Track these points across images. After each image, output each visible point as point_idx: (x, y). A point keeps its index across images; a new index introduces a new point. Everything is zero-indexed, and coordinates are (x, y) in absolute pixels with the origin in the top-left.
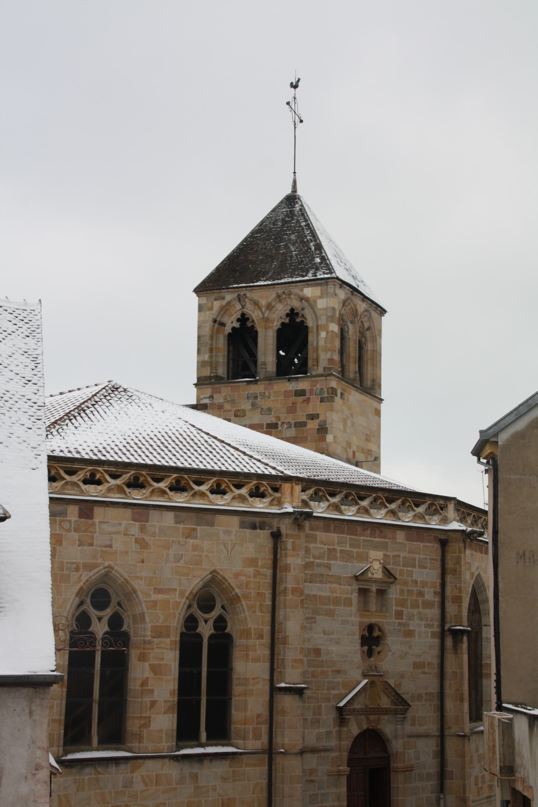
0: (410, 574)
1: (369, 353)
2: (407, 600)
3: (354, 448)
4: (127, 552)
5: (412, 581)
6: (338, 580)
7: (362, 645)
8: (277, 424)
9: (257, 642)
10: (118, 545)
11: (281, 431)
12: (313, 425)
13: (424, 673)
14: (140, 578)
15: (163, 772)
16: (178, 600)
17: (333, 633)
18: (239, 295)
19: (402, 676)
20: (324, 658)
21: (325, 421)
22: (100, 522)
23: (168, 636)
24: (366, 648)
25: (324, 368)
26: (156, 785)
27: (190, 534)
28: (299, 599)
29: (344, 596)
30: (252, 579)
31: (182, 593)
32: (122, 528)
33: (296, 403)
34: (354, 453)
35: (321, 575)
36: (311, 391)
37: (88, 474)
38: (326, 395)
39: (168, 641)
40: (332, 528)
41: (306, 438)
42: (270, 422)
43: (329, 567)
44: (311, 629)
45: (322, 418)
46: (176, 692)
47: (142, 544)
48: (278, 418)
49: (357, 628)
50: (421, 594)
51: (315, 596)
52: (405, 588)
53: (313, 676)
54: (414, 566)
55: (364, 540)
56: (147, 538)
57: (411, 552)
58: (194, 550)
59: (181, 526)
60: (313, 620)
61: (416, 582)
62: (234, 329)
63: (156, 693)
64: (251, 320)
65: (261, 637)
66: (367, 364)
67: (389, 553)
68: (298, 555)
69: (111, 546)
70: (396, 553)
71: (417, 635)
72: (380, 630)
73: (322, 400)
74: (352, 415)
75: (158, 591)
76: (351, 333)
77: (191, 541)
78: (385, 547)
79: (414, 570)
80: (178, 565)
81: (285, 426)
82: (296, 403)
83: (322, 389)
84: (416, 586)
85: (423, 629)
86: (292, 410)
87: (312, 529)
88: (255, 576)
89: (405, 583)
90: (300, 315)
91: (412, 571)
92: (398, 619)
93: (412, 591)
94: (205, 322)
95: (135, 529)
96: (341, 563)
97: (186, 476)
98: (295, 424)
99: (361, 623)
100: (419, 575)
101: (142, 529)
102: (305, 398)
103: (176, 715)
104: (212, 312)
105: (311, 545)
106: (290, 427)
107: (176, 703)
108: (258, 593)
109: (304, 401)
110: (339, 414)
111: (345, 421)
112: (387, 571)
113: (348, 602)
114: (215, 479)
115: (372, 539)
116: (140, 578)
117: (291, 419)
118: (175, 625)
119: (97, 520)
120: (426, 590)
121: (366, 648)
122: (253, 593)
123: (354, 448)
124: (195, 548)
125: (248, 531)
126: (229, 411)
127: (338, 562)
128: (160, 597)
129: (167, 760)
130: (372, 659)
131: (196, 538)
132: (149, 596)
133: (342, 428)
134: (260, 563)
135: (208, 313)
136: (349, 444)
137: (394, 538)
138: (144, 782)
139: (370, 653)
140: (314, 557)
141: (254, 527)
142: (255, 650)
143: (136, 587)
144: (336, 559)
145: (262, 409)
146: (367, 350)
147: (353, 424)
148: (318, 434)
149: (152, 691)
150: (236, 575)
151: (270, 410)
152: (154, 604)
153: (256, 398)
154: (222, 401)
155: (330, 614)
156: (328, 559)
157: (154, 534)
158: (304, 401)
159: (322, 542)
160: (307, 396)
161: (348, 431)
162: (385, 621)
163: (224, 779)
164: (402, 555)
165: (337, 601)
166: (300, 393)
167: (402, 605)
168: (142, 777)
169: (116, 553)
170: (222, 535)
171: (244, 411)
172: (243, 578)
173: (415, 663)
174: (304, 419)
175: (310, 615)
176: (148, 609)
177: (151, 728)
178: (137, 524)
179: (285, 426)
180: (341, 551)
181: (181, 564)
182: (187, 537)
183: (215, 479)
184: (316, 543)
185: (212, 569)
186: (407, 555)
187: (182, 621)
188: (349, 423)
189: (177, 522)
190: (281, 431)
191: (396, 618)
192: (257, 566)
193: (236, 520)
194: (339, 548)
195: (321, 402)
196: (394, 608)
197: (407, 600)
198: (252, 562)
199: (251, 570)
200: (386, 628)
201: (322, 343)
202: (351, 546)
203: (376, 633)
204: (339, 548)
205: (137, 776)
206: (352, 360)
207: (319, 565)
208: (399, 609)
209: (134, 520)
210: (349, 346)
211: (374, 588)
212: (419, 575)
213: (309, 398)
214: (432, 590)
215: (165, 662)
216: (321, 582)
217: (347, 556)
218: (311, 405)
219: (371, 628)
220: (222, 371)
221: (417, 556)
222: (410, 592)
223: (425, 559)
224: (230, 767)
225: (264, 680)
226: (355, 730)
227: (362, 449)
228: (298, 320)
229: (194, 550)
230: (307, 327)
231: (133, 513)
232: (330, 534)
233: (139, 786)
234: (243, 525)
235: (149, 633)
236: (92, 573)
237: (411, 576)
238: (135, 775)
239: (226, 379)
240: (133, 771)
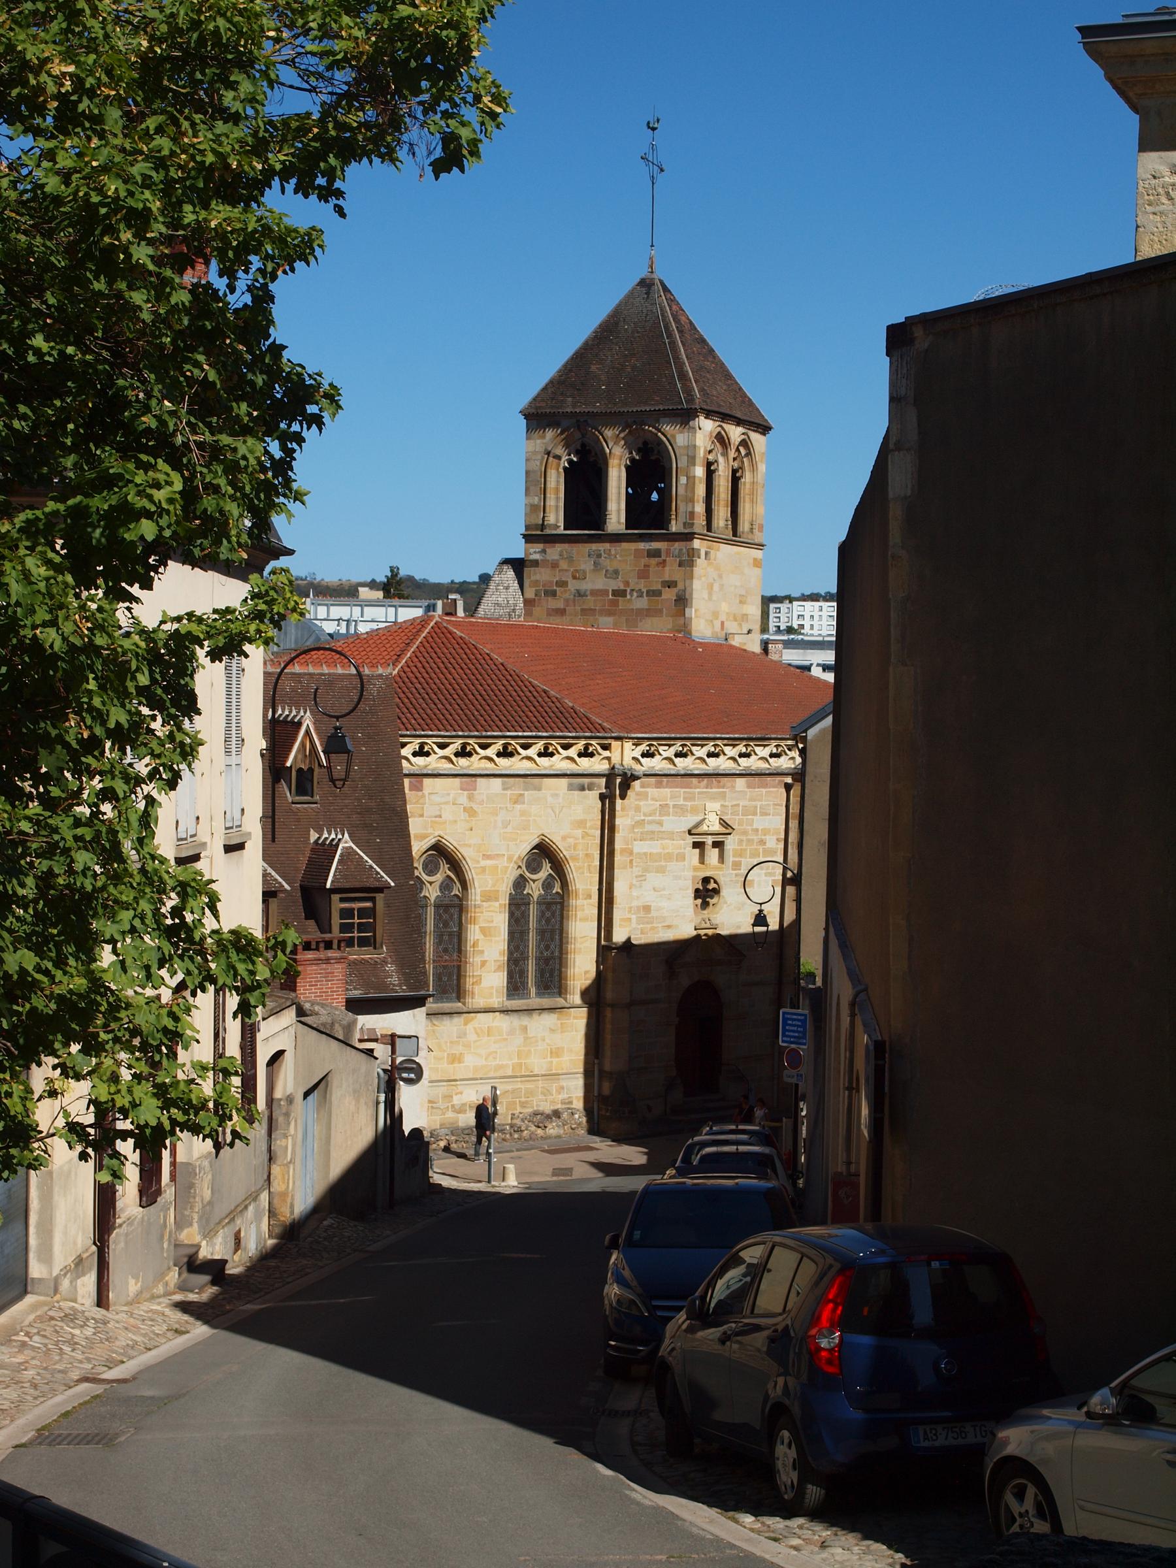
0: (751, 823)
1: (748, 486)
2: (746, 850)
3: (723, 617)
4: (456, 821)
5: (752, 830)
6: (671, 835)
7: (696, 898)
8: (626, 590)
9: (585, 902)
10: (447, 815)
11: (630, 600)
12: (669, 595)
14: (470, 846)
15: (494, 1025)
16: (506, 864)
17: (664, 889)
18: (578, 421)
20: (653, 914)
21: (684, 591)
22: (430, 794)
23: (497, 899)
24: (699, 901)
25: (685, 524)
26: (488, 1035)
27: (518, 800)
28: (628, 859)
29: (676, 852)
30: (581, 841)
31: (510, 858)
32: (451, 798)
33: (648, 566)
34: (722, 623)
35: (653, 832)
36: (668, 552)
37: (417, 747)
38: (685, 558)
39: (497, 904)
40: (664, 783)
41: (661, 611)
42: (616, 588)
43: (660, 823)
44: (641, 887)
45: (680, 586)
46: (506, 952)
47: (471, 812)
48: (627, 584)
49: (690, 882)
50: (762, 842)
51: (645, 854)
52: (744, 838)
53: (642, 933)
54: (755, 814)
56: (475, 807)
57: (751, 800)
58: (521, 815)
59: (509, 792)
60: (643, 878)
61: (757, 830)
62: (570, 462)
63: (486, 953)
64: (593, 454)
65: (590, 897)
66: (744, 502)
67: (727, 803)
68: (628, 815)
69: (440, 816)
70: (735, 803)
71: (755, 885)
72: (715, 882)
73: (680, 566)
74: (720, 576)
75: (487, 857)
76: (721, 468)
77: (518, 807)
78: (723, 796)
79: (755, 818)
80: (505, 830)
81: (635, 594)
82: (648, 566)
83: (681, 550)
84: (757, 835)
85: (764, 878)
86: (643, 574)
87: (642, 786)
88: (583, 837)
89: (745, 833)
90: (656, 452)
91: (753, 820)
92: (735, 870)
93: (753, 840)
94: (535, 452)
95: (463, 798)
96: (674, 818)
97: (512, 742)
98: (648, 592)
99: (694, 878)
100: (760, 822)
101: (470, 798)
102: (660, 560)
103: (506, 973)
104: (544, 441)
105: (642, 803)
106: (641, 596)
107: (506, 962)
108: (587, 855)
109: (658, 564)
110: (703, 579)
111: (710, 587)
112: (724, 823)
113: (681, 857)
114: (543, 742)
115: (709, 790)
116: (470, 846)
117: (642, 585)
118: (504, 889)
119: (426, 791)
120: (767, 837)
121: (699, 901)
122: (581, 854)
123: (723, 617)
124: (523, 813)
125: (576, 792)
126: (567, 570)
127: (671, 817)
128: (488, 862)
129: (497, 1014)
130: (705, 912)
131: (524, 803)
132: (478, 862)
133: (706, 596)
134: (588, 825)
135: (538, 441)
136: (716, 614)
137: (733, 787)
138: (477, 1033)
139: (705, 905)
140: (645, 815)
141: (582, 789)
142: (583, 910)
143: (465, 855)
144: (669, 815)
145: (607, 571)
146: (745, 483)
147: (722, 586)
148: (675, 605)
149: (482, 952)
150: (564, 838)
151: (616, 572)
152: (483, 869)
153: (599, 556)
154: (556, 557)
155: (661, 870)
156: (660, 815)
157: (482, 802)
158: (658, 564)
159: (653, 799)
160: (663, 557)
161: (714, 598)
162: (721, 873)
163: (552, 1031)
164: (741, 804)
165: (668, 857)
166: (656, 554)
167: (741, 856)
168: (475, 1028)
169: (445, 823)
170: (550, 799)
171: (584, 572)
172: (571, 840)
174: (659, 587)
175: (640, 873)
176: (477, 874)
177: (482, 985)
178: (466, 792)
179: (635, 594)
180: (674, 806)
181: (509, 829)
182: (515, 803)
183: (543, 742)
184: (647, 800)
185: (540, 833)
186: (746, 803)
187: (511, 884)
188: (716, 587)
189: (504, 789)
190: (630, 600)
191: (733, 869)
192: (585, 828)
193: (564, 782)
194: (671, 804)
195: (680, 566)
196: (731, 859)
197: (746, 850)
198: (581, 824)
199: (579, 833)
200: (721, 880)
201: (681, 491)
202: (685, 799)
203: (712, 885)
204: (671, 804)
205: (470, 1027)
206: (722, 503)
207: (650, 822)
208: (737, 859)
209: (462, 789)
210: (719, 485)
211: (709, 840)
212: (760, 822)
213: (664, 561)
214: (775, 837)
215: (494, 924)
216: (652, 839)
217: (681, 810)
218: (667, 568)
219: (706, 880)
220: (556, 517)
221: (759, 804)
222: (750, 841)
223: (769, 805)
224: (558, 1019)
225: (592, 938)
226: (685, 981)
227: (734, 615)
228: (653, 458)
229: (521, 815)
230: (663, 467)
231: (461, 783)
232: (662, 790)
233: (472, 1037)
234: (571, 788)
235: (478, 898)
236: (423, 843)
237: (752, 825)
238: (468, 1027)
239: (562, 528)
240: (466, 1024)
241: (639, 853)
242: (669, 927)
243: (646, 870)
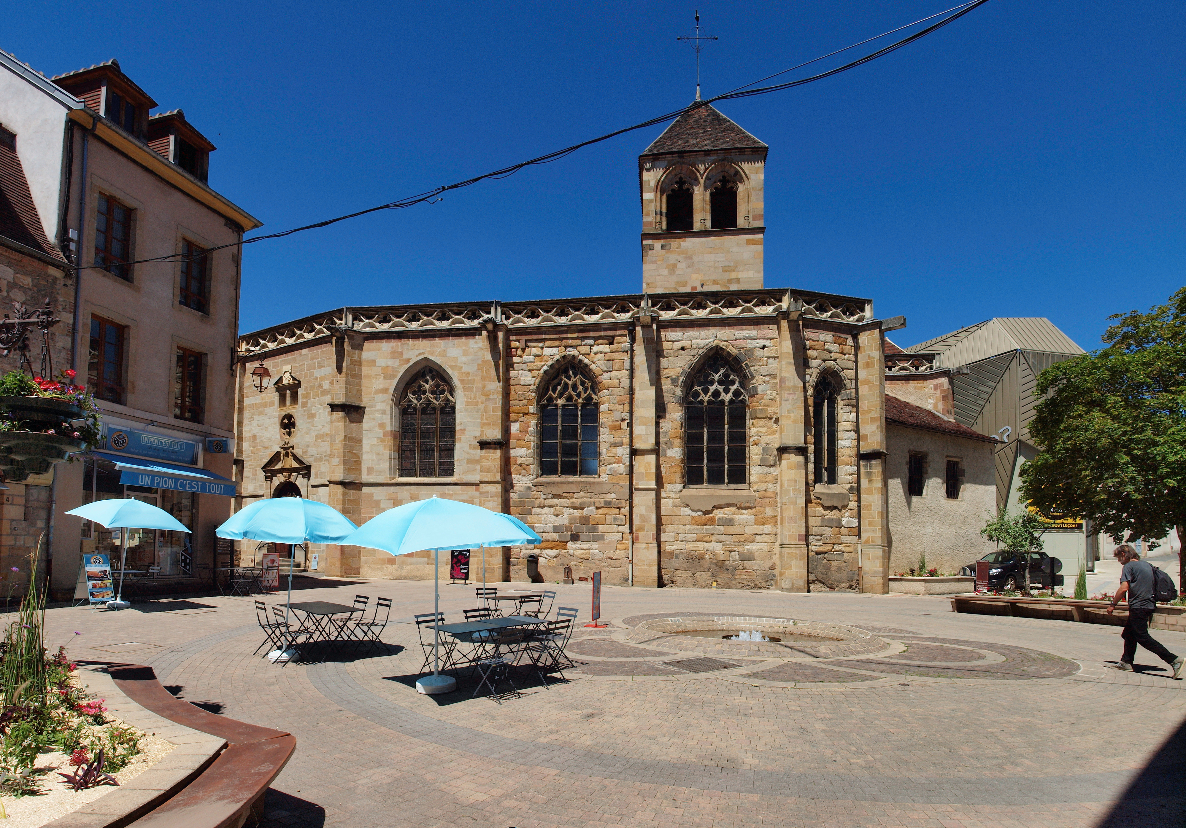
2: (310, 393)
13: (322, 441)
19: (308, 446)
20: (258, 440)
29: (269, 401)
51: (253, 404)
54: (314, 368)
55: (281, 361)
61: (317, 379)
67: (297, 365)
93: (314, 386)
99: (279, 415)
155: (261, 414)
167: (306, 397)
173: (316, 436)
191: (302, 407)
241: (250, 405)
242: (266, 448)
243: (254, 415)
